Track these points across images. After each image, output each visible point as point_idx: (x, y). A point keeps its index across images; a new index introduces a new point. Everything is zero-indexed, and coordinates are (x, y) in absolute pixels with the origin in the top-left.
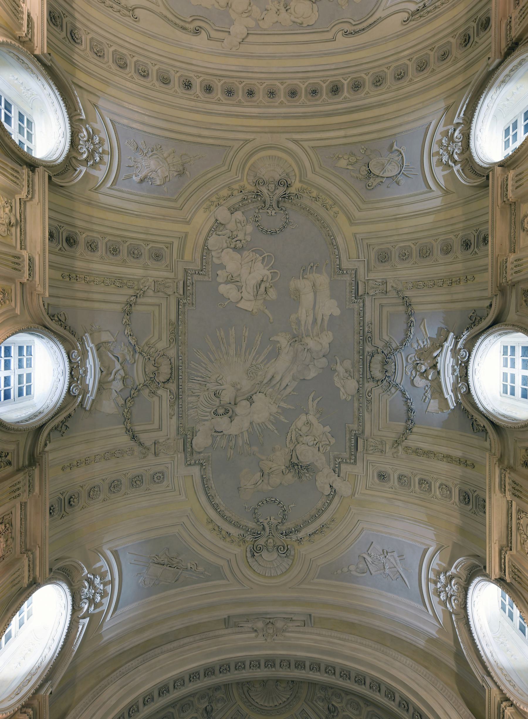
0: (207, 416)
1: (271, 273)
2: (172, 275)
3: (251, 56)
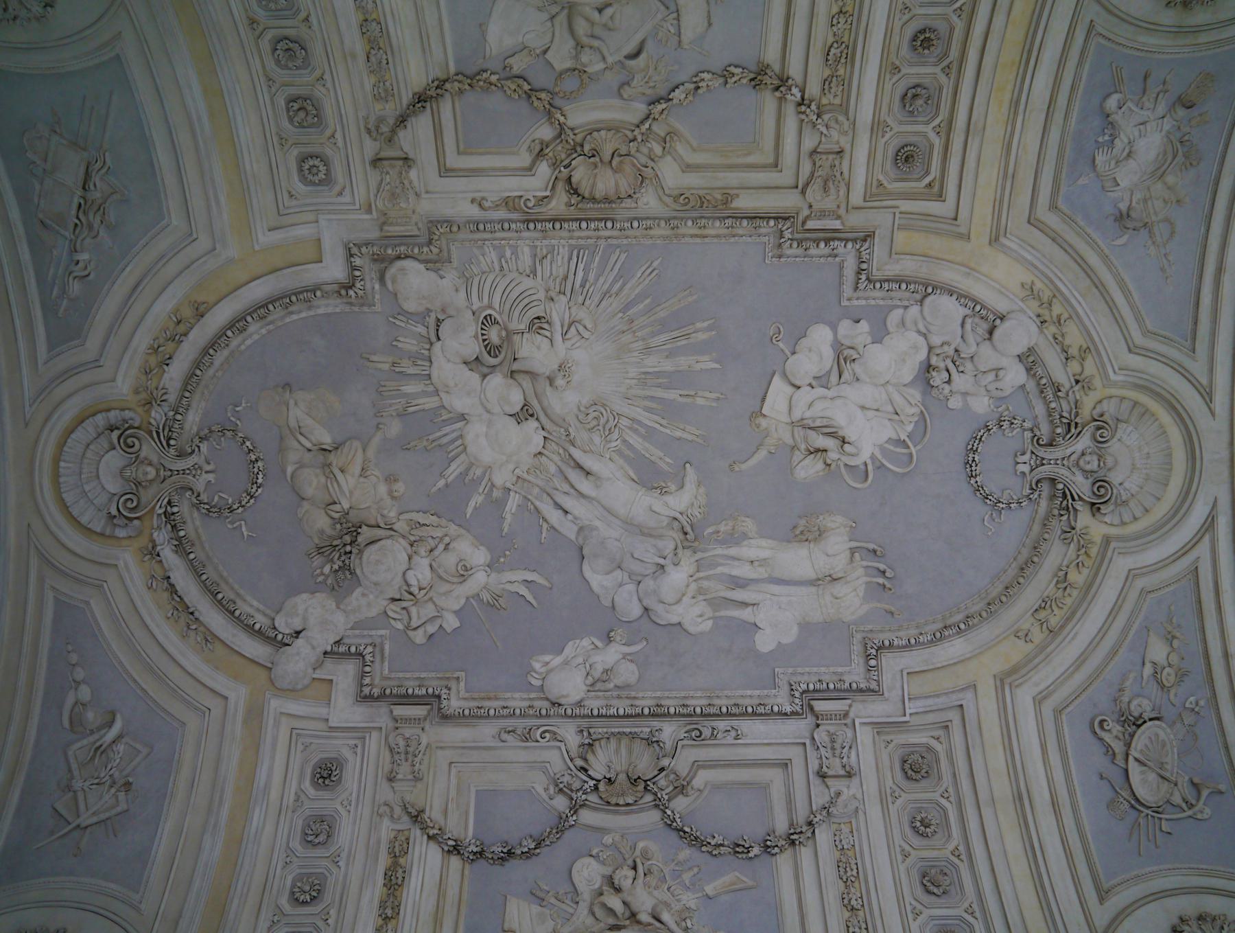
0: (480, 298)
1: (866, 464)
2: (856, 198)
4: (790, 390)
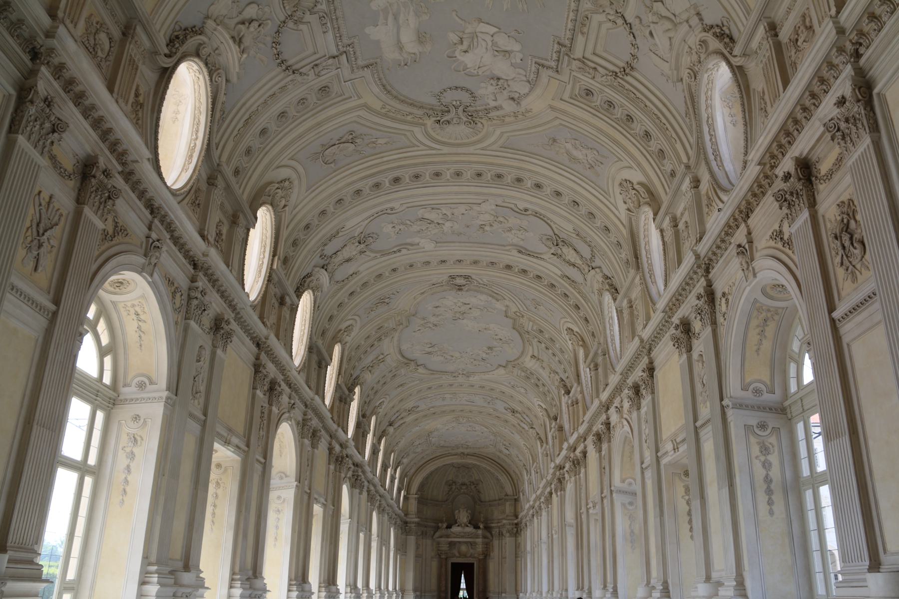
4: (491, 33)
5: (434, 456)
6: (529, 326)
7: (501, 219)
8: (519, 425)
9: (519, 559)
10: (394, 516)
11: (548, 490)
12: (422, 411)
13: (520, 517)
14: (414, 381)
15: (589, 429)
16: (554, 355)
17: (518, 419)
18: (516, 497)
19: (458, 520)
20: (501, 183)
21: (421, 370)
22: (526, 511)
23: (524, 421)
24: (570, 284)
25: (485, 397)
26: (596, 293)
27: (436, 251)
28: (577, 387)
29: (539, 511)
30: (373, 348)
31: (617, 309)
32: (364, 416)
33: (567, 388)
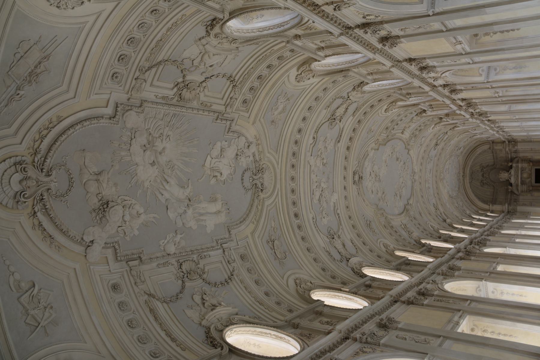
0: (148, 126)
3: (304, 168)
4: (211, 159)
5: (465, 194)
6: (384, 136)
7: (319, 153)
8: (445, 141)
9: (532, 139)
10: (504, 220)
11: (486, 122)
12: (436, 202)
13: (504, 140)
14: (418, 206)
15: (448, 97)
16: (401, 120)
17: (441, 141)
18: (491, 142)
19: (506, 179)
20: (298, 153)
21: (411, 202)
22: (500, 136)
23: (442, 138)
24: (358, 111)
25: (427, 163)
26: (364, 95)
27: (338, 192)
28: (421, 105)
29: (500, 127)
30: (397, 231)
31: (373, 82)
32: (440, 237)
33: (422, 112)
